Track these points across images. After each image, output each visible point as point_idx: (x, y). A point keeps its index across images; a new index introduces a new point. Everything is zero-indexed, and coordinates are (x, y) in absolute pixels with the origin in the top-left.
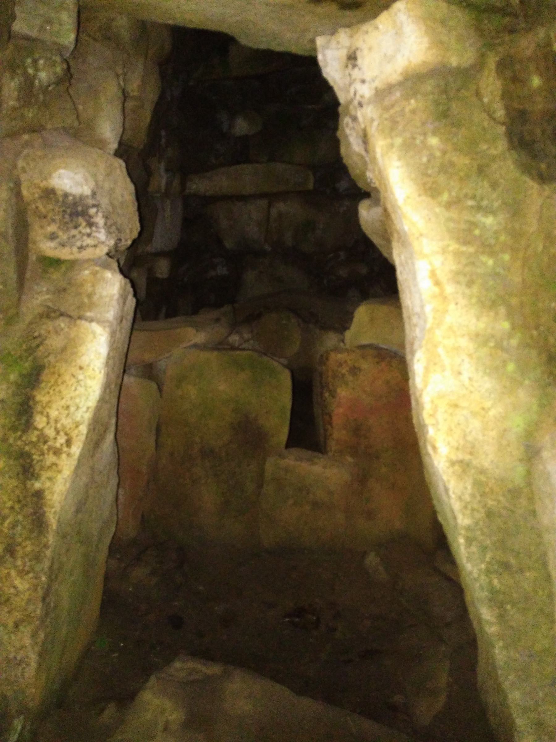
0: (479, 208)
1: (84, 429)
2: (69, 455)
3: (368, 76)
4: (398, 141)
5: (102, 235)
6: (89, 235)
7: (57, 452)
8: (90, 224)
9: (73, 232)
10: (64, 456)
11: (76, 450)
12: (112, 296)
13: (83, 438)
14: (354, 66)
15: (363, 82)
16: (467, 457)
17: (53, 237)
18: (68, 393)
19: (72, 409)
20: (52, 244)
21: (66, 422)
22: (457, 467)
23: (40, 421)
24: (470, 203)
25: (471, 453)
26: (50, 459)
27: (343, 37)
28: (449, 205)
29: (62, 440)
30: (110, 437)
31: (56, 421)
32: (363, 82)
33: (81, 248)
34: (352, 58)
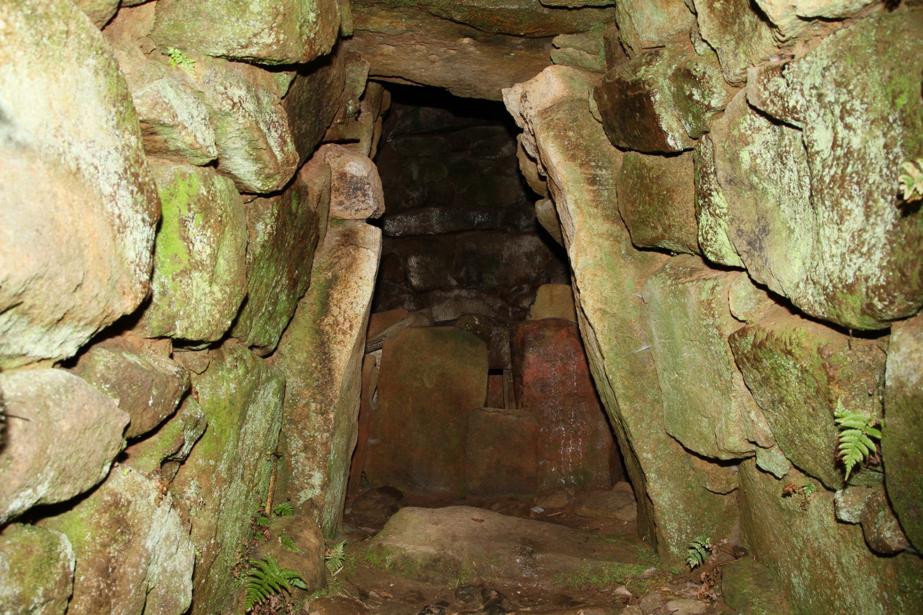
0: (597, 166)
1: (360, 319)
2: (351, 335)
3: (533, 105)
4: (552, 133)
5: (371, 202)
6: (363, 202)
7: (344, 333)
8: (365, 195)
9: (354, 200)
10: (348, 336)
11: (356, 332)
12: (376, 240)
13: (360, 325)
14: (526, 101)
15: (531, 108)
16: (603, 307)
17: (341, 203)
18: (352, 294)
19: (354, 305)
20: (340, 208)
21: (350, 313)
22: (598, 313)
23: (335, 310)
24: (593, 164)
25: (606, 304)
26: (340, 337)
27: (519, 88)
28: (581, 165)
29: (347, 325)
30: (364, 346)
31: (345, 312)
32: (531, 108)
33: (357, 210)
34: (524, 97)
